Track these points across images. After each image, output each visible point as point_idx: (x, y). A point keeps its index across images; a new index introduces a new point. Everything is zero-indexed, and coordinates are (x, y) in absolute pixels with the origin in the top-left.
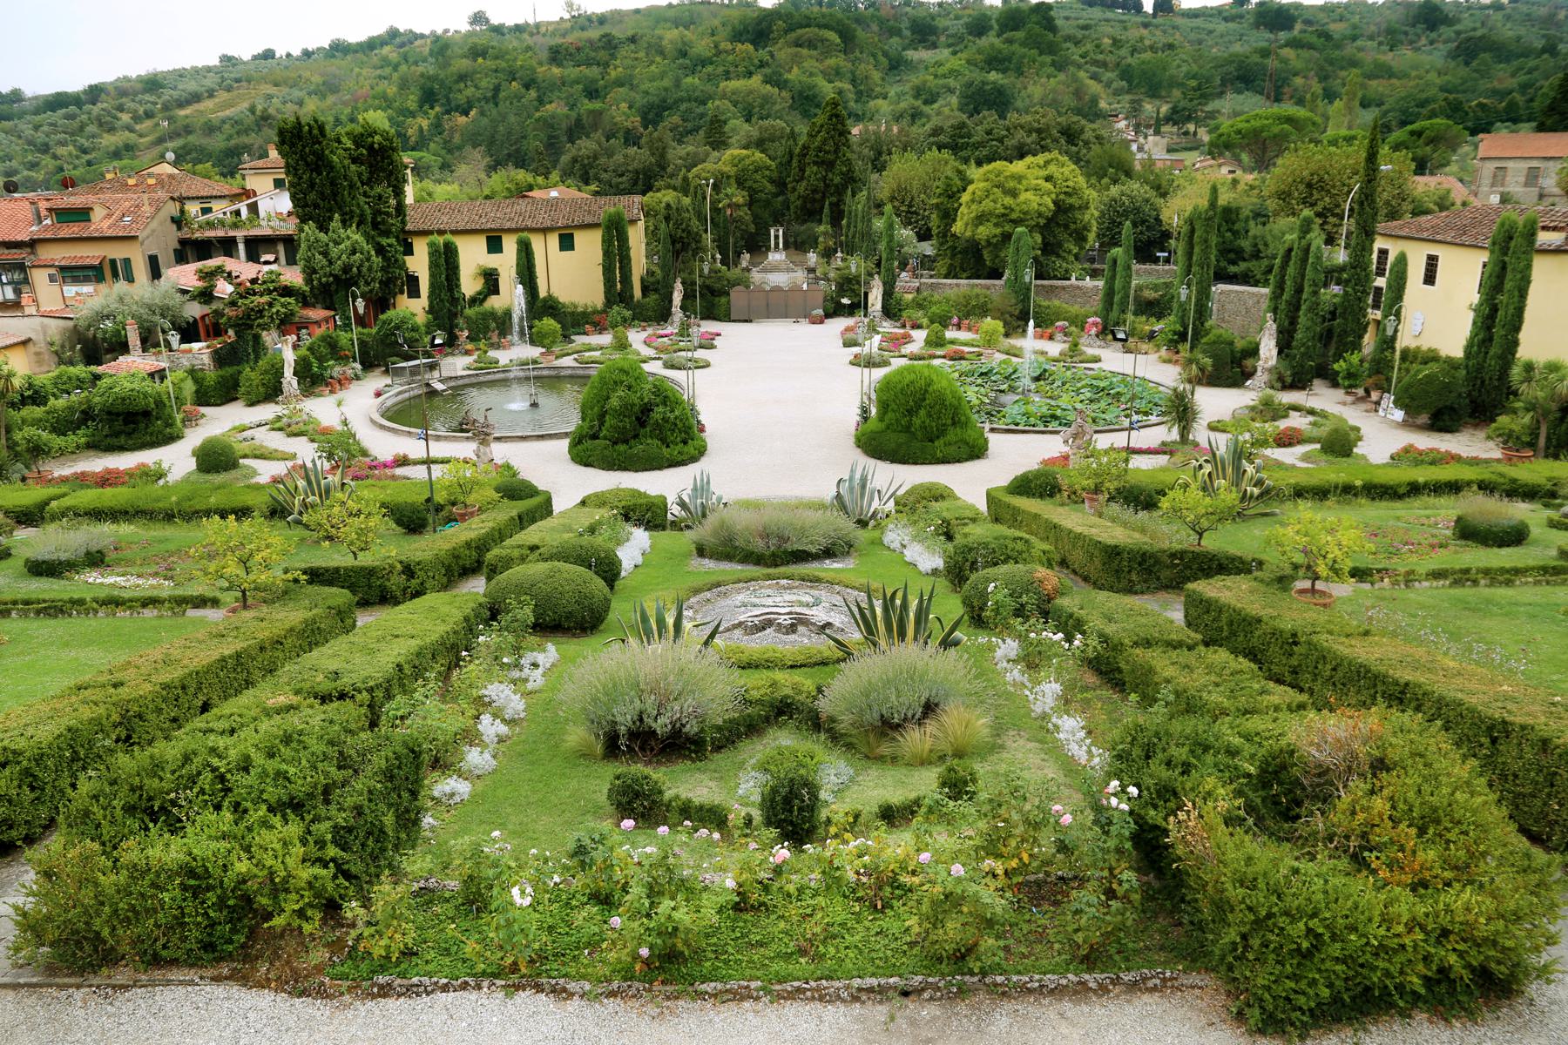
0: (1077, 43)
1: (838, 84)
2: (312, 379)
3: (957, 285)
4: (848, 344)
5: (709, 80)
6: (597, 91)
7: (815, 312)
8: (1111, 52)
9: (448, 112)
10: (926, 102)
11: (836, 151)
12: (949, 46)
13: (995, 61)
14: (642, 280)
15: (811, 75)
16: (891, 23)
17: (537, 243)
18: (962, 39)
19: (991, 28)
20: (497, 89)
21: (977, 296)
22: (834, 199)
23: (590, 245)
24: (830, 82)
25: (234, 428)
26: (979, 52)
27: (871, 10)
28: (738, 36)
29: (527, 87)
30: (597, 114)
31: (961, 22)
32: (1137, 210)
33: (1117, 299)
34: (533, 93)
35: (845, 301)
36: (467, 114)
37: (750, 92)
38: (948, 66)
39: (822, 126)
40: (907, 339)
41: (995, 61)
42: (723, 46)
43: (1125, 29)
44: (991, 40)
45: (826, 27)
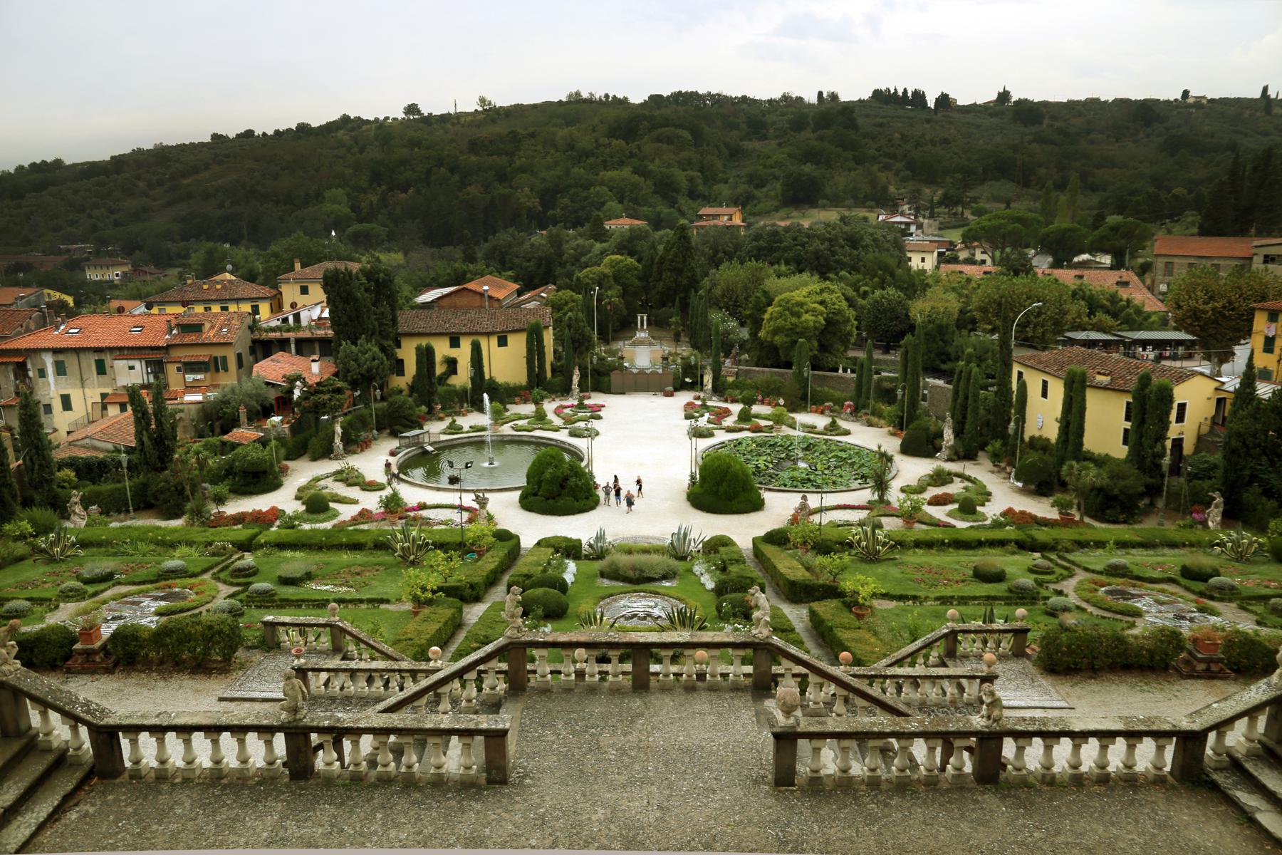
2: (354, 443)
3: (763, 372)
4: (688, 417)
7: (668, 389)
10: (758, 187)
11: (684, 262)
12: (776, 137)
13: (810, 156)
14: (552, 365)
15: (669, 166)
17: (484, 343)
21: (775, 381)
22: (682, 295)
23: (518, 343)
24: (684, 170)
25: (313, 480)
28: (613, 133)
32: (893, 311)
33: (864, 389)
35: (688, 380)
40: (727, 413)
41: (810, 156)
42: (604, 140)
44: (807, 134)
45: (681, 127)
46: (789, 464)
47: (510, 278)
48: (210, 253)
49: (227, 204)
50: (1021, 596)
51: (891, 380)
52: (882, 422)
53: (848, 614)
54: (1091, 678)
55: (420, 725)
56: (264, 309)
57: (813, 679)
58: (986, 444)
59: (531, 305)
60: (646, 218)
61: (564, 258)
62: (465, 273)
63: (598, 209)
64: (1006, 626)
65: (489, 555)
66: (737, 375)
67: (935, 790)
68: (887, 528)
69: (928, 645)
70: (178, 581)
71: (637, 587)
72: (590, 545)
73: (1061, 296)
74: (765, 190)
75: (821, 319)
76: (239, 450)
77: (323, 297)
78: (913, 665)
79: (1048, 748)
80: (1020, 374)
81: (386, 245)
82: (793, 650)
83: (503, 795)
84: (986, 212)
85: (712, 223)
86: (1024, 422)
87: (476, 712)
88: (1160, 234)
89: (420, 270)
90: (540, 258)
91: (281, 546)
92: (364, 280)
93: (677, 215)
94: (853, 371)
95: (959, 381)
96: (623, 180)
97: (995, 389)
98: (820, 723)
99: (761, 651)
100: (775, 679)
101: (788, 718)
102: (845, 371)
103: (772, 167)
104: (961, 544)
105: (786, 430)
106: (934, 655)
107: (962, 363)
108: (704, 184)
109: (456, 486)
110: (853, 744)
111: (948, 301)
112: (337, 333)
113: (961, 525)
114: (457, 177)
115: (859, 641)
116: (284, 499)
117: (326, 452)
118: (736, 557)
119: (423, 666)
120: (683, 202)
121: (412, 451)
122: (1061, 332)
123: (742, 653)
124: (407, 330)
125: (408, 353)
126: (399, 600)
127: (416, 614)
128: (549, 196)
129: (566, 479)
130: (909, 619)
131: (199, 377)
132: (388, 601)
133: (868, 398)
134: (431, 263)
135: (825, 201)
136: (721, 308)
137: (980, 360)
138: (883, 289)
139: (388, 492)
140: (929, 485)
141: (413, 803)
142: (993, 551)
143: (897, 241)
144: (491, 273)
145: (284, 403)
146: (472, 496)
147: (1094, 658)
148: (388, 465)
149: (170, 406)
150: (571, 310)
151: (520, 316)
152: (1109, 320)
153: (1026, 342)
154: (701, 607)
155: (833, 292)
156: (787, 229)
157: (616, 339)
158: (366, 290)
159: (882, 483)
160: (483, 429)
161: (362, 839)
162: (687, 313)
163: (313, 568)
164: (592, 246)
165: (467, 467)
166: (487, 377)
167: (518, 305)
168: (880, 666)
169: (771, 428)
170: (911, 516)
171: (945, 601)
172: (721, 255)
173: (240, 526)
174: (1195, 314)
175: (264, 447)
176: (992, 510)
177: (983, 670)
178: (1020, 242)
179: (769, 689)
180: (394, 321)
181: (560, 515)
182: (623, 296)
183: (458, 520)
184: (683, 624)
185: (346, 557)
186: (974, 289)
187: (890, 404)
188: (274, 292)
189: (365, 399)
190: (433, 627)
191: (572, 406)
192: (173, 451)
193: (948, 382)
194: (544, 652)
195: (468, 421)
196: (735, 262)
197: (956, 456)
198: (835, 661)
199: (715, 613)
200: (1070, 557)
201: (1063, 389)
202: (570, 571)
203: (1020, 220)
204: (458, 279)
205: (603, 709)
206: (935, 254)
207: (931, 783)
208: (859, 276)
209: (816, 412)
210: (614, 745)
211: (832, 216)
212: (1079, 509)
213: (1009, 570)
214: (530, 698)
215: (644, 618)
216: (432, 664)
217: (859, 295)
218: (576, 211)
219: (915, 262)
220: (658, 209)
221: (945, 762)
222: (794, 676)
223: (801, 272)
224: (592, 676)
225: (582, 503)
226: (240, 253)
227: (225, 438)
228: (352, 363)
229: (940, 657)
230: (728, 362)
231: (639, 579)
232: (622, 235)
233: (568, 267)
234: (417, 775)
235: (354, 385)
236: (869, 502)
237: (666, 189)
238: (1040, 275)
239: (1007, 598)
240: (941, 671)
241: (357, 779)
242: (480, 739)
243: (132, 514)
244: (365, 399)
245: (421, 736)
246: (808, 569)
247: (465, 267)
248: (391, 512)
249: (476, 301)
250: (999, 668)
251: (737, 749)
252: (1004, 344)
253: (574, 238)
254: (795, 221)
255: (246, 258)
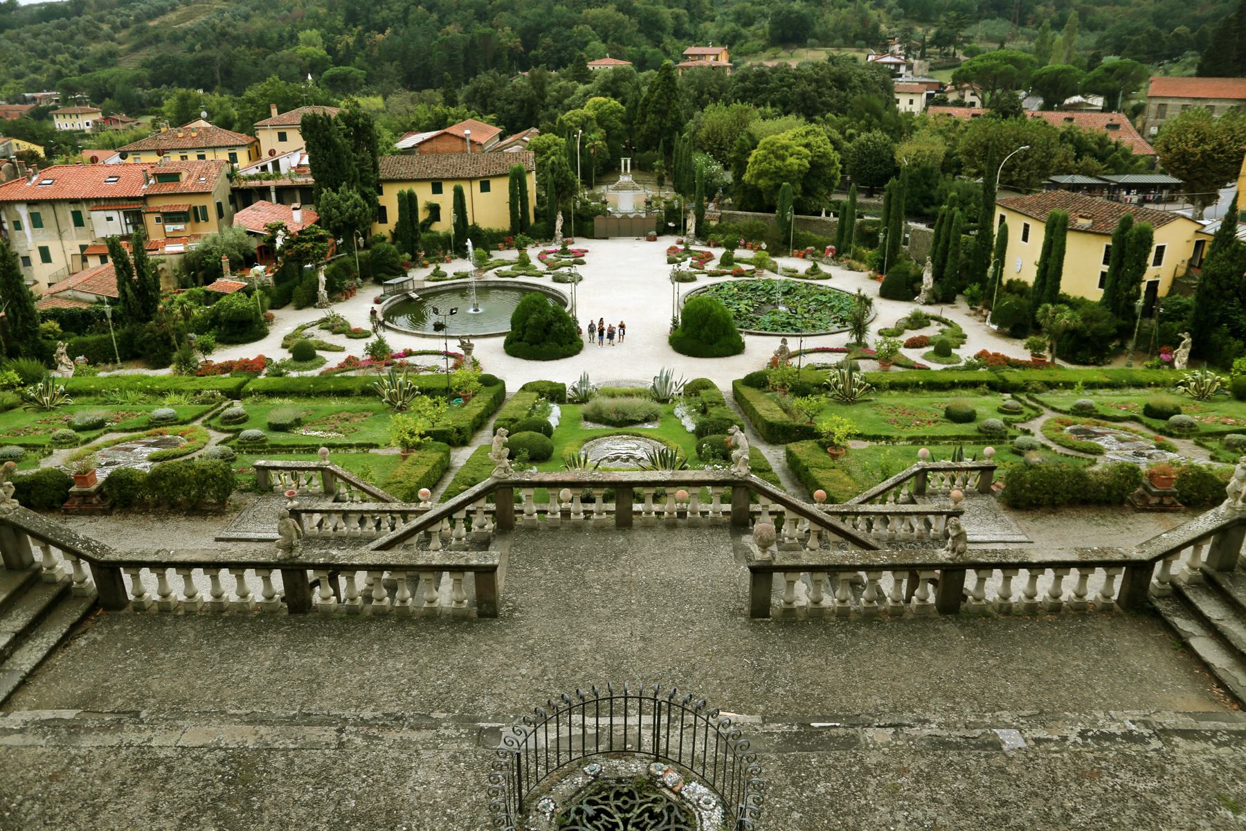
2: (338, 291)
4: (670, 262)
11: (669, 103)
14: (535, 210)
17: (466, 188)
22: (666, 138)
23: (501, 188)
24: (670, 7)
32: (879, 153)
33: (846, 233)
35: (671, 224)
40: (710, 257)
46: (769, 308)
47: (492, 122)
48: (183, 99)
49: (198, 47)
50: (990, 435)
51: (873, 223)
52: (863, 266)
53: (823, 454)
54: (1050, 513)
55: (412, 562)
56: (242, 155)
57: (789, 515)
58: (964, 287)
59: (514, 149)
60: (631, 58)
61: (548, 100)
62: (446, 117)
63: (581, 49)
64: (974, 464)
65: (474, 400)
66: (720, 219)
67: (900, 620)
68: (863, 370)
69: (899, 484)
70: (169, 428)
71: (620, 430)
72: (574, 389)
73: (1049, 139)
74: (752, 28)
75: (806, 162)
76: (224, 300)
77: (303, 144)
78: (883, 502)
79: (1007, 579)
80: (1002, 218)
81: (365, 89)
82: (770, 488)
83: (493, 628)
84: (979, 52)
85: (698, 63)
86: (1003, 265)
87: (466, 550)
88: (1157, 75)
89: (399, 114)
90: (522, 101)
91: (270, 393)
92: (343, 126)
93: (662, 54)
94: (835, 215)
95: (940, 225)
96: (607, 18)
97: (976, 232)
98: (794, 557)
99: (741, 490)
100: (753, 516)
101: (764, 552)
102: (828, 214)
104: (935, 386)
105: (767, 275)
106: (905, 492)
107: (944, 207)
108: (691, 22)
109: (441, 333)
110: (824, 577)
111: (934, 144)
112: (317, 180)
113: (935, 367)
114: (435, 16)
115: (832, 480)
116: (271, 348)
117: (311, 301)
118: (716, 399)
119: (413, 507)
120: (668, 41)
121: (397, 298)
122: (1046, 176)
123: (721, 490)
124: (389, 176)
125: (390, 199)
126: (388, 445)
127: (405, 458)
128: (530, 36)
129: (550, 324)
130: (882, 458)
131: (180, 227)
132: (377, 446)
133: (850, 242)
134: (411, 107)
135: (814, 41)
136: (705, 152)
137: (963, 204)
138: (870, 131)
139: (373, 339)
140: (906, 328)
141: (408, 636)
142: (965, 392)
143: (885, 82)
144: (472, 117)
145: (266, 252)
146: (458, 342)
147: (1056, 494)
148: (373, 313)
149: (152, 257)
150: (553, 154)
151: (503, 161)
152: (1095, 164)
153: (1011, 186)
154: (682, 447)
155: (818, 134)
156: (774, 70)
157: (599, 183)
158: (346, 136)
159: (860, 326)
160: (465, 276)
161: (361, 669)
162: (671, 157)
163: (302, 415)
164: (575, 88)
165: (452, 313)
166: (470, 223)
167: (500, 150)
168: (853, 503)
169: (753, 272)
170: (887, 358)
171: (917, 441)
172: (706, 96)
173: (228, 375)
174: (1184, 157)
175: (249, 296)
176: (965, 353)
177: (950, 506)
178: (1010, 83)
179: (747, 525)
180: (375, 167)
181: (544, 360)
182: (607, 139)
183: (444, 367)
184: (664, 465)
185: (334, 404)
186: (962, 132)
187: (871, 248)
188: (251, 139)
189: (347, 247)
190: (422, 470)
191: (556, 251)
192: (157, 302)
193: (930, 227)
194: (531, 492)
195: (454, 267)
196: (721, 104)
197: (935, 299)
198: (811, 500)
199: (696, 454)
200: (1039, 397)
201: (1043, 233)
202: (555, 413)
203: (1013, 60)
204: (440, 123)
205: (588, 546)
206: (924, 96)
207: (897, 614)
208: (846, 119)
209: (798, 256)
210: (598, 580)
211: (820, 55)
212: (1051, 351)
213: (979, 410)
214: (517, 535)
215: (627, 460)
216: (422, 505)
217: (845, 138)
218: (559, 51)
219: (903, 105)
220: (643, 48)
221: (910, 593)
222: (771, 513)
223: (787, 114)
224: (577, 514)
225: (565, 349)
226: (215, 99)
227: (209, 288)
228: (334, 211)
229: (909, 494)
230: (711, 206)
231: (622, 422)
232: (606, 76)
233: (551, 110)
234: (411, 609)
235: (337, 233)
236: (847, 345)
237: (651, 27)
238: (1029, 118)
239: (976, 438)
240: (910, 508)
241: (353, 613)
242: (470, 575)
243: (119, 364)
244: (347, 247)
245: (414, 573)
246: (786, 411)
247: (445, 111)
248: (378, 359)
249: (458, 145)
250: (965, 504)
251: (715, 583)
252: (988, 188)
253: (556, 80)
254: (782, 61)
255: (221, 104)
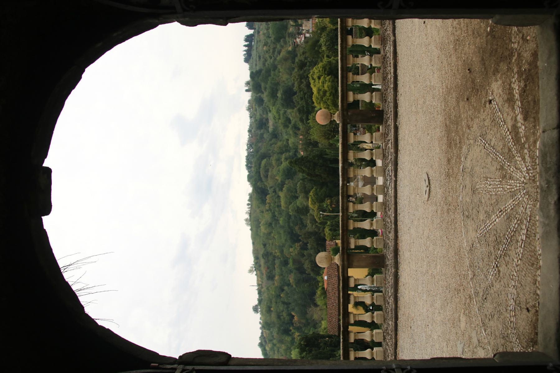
0: (266, 60)
1: (283, 160)
5: (281, 214)
6: (285, 261)
8: (269, 46)
9: (293, 324)
10: (290, 122)
12: (267, 113)
15: (279, 171)
16: (258, 138)
18: (264, 108)
19: (260, 96)
20: (284, 303)
24: (282, 163)
26: (270, 101)
27: (253, 146)
28: (263, 202)
29: (283, 290)
30: (294, 261)
31: (258, 108)
34: (286, 288)
36: (293, 316)
37: (286, 197)
38: (275, 114)
39: (300, 168)
41: (273, 95)
42: (267, 208)
43: (260, 41)
45: (260, 164)
103: (279, 115)
